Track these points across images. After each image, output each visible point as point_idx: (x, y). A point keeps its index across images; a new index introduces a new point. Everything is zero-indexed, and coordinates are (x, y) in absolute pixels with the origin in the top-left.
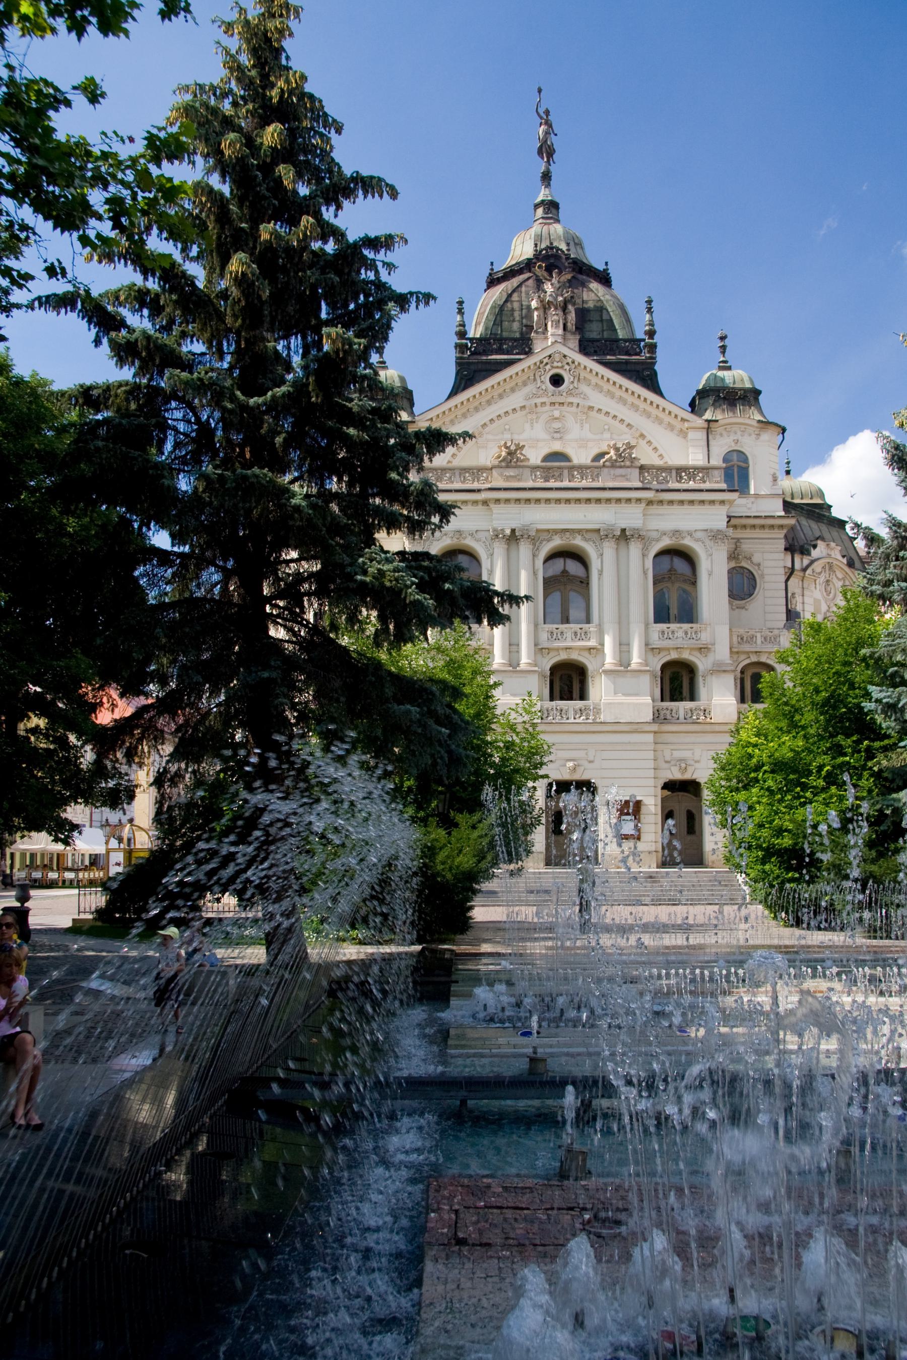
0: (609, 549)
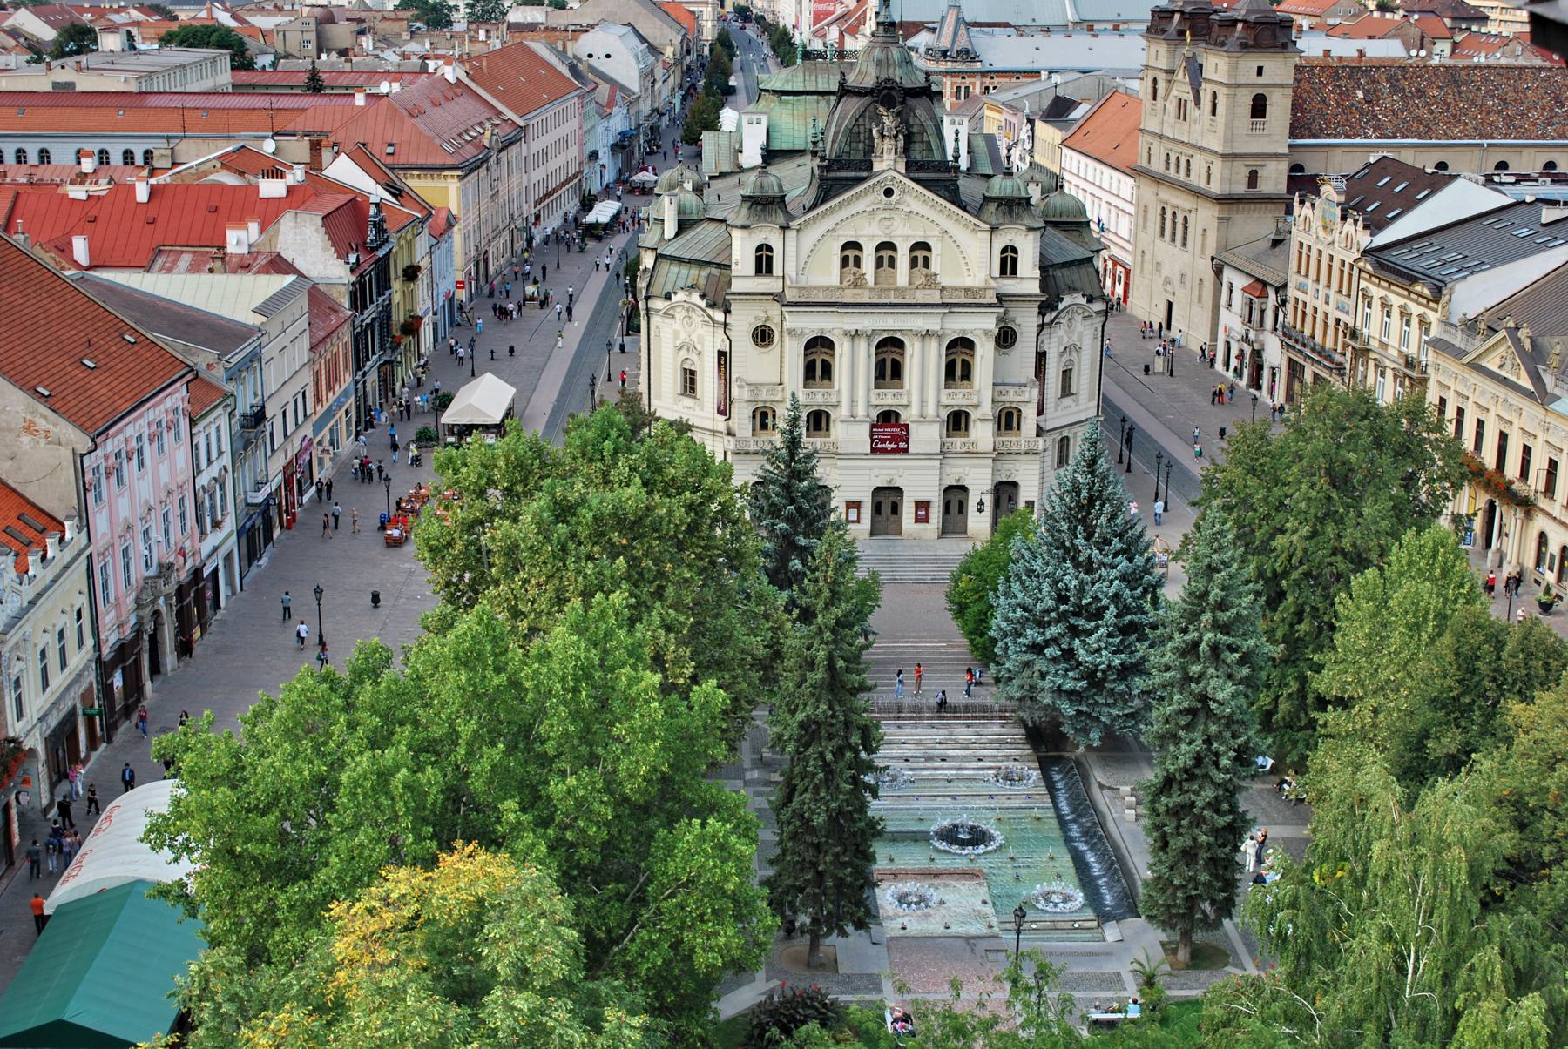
0: (917, 344)
